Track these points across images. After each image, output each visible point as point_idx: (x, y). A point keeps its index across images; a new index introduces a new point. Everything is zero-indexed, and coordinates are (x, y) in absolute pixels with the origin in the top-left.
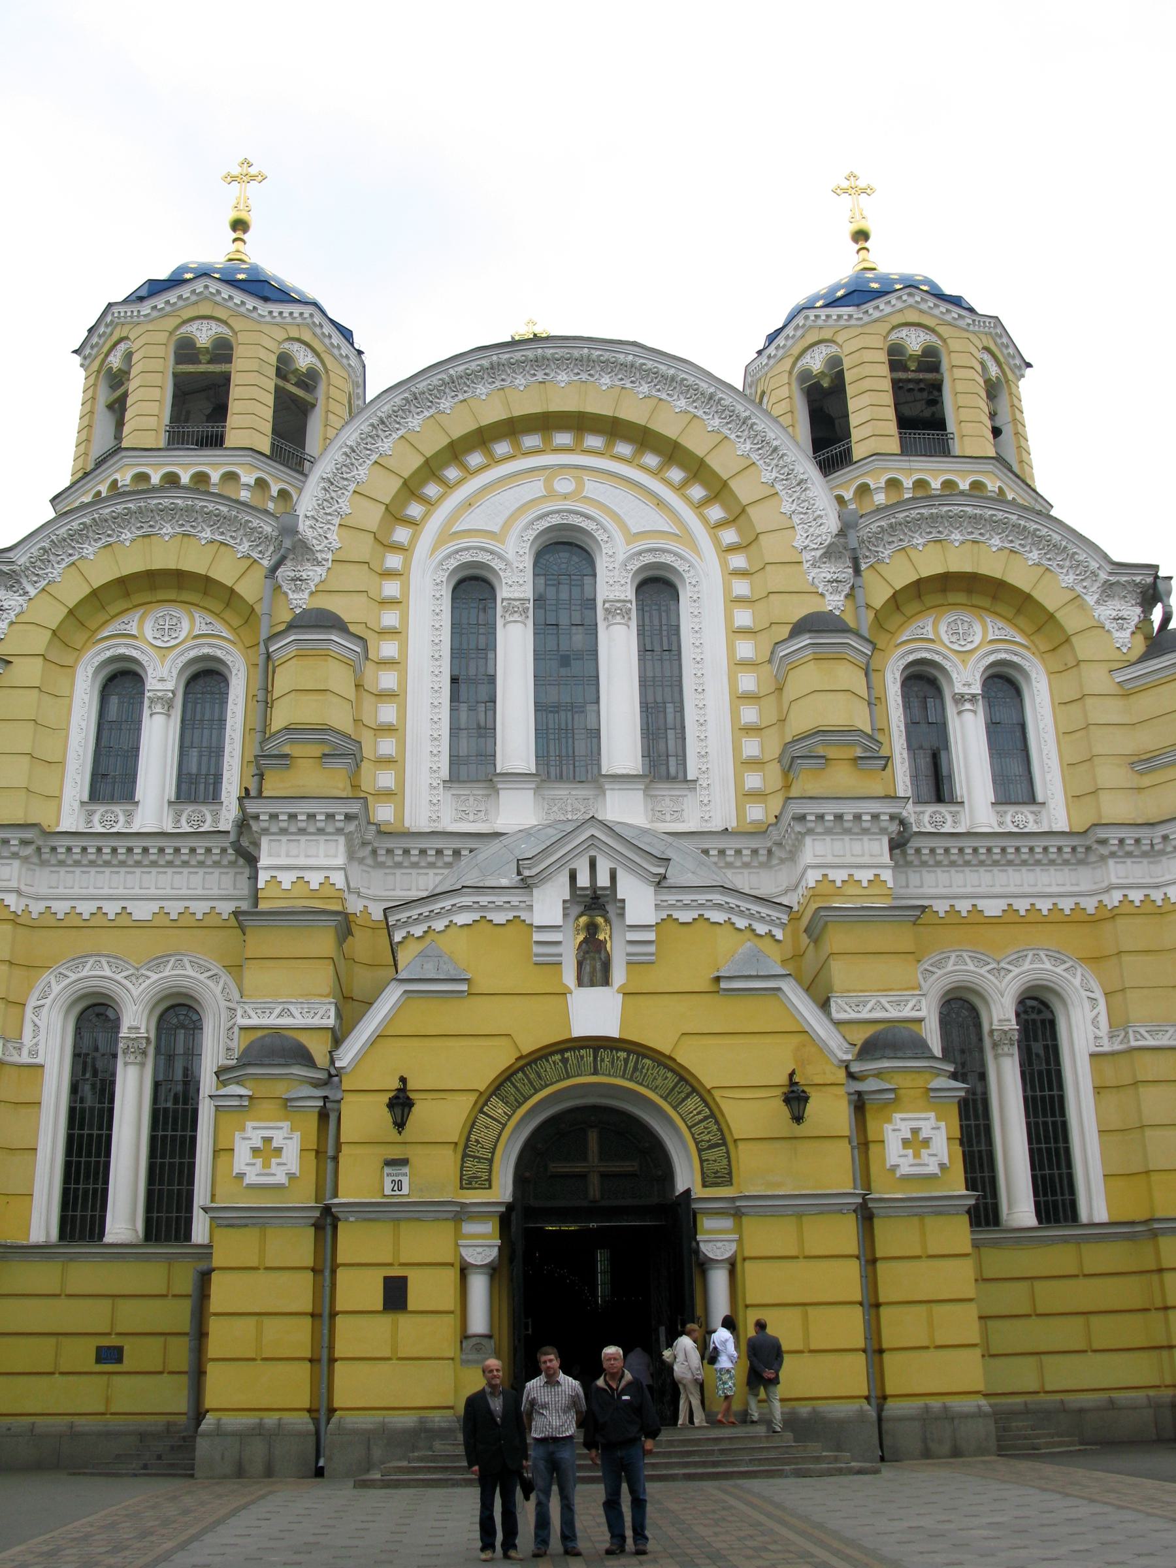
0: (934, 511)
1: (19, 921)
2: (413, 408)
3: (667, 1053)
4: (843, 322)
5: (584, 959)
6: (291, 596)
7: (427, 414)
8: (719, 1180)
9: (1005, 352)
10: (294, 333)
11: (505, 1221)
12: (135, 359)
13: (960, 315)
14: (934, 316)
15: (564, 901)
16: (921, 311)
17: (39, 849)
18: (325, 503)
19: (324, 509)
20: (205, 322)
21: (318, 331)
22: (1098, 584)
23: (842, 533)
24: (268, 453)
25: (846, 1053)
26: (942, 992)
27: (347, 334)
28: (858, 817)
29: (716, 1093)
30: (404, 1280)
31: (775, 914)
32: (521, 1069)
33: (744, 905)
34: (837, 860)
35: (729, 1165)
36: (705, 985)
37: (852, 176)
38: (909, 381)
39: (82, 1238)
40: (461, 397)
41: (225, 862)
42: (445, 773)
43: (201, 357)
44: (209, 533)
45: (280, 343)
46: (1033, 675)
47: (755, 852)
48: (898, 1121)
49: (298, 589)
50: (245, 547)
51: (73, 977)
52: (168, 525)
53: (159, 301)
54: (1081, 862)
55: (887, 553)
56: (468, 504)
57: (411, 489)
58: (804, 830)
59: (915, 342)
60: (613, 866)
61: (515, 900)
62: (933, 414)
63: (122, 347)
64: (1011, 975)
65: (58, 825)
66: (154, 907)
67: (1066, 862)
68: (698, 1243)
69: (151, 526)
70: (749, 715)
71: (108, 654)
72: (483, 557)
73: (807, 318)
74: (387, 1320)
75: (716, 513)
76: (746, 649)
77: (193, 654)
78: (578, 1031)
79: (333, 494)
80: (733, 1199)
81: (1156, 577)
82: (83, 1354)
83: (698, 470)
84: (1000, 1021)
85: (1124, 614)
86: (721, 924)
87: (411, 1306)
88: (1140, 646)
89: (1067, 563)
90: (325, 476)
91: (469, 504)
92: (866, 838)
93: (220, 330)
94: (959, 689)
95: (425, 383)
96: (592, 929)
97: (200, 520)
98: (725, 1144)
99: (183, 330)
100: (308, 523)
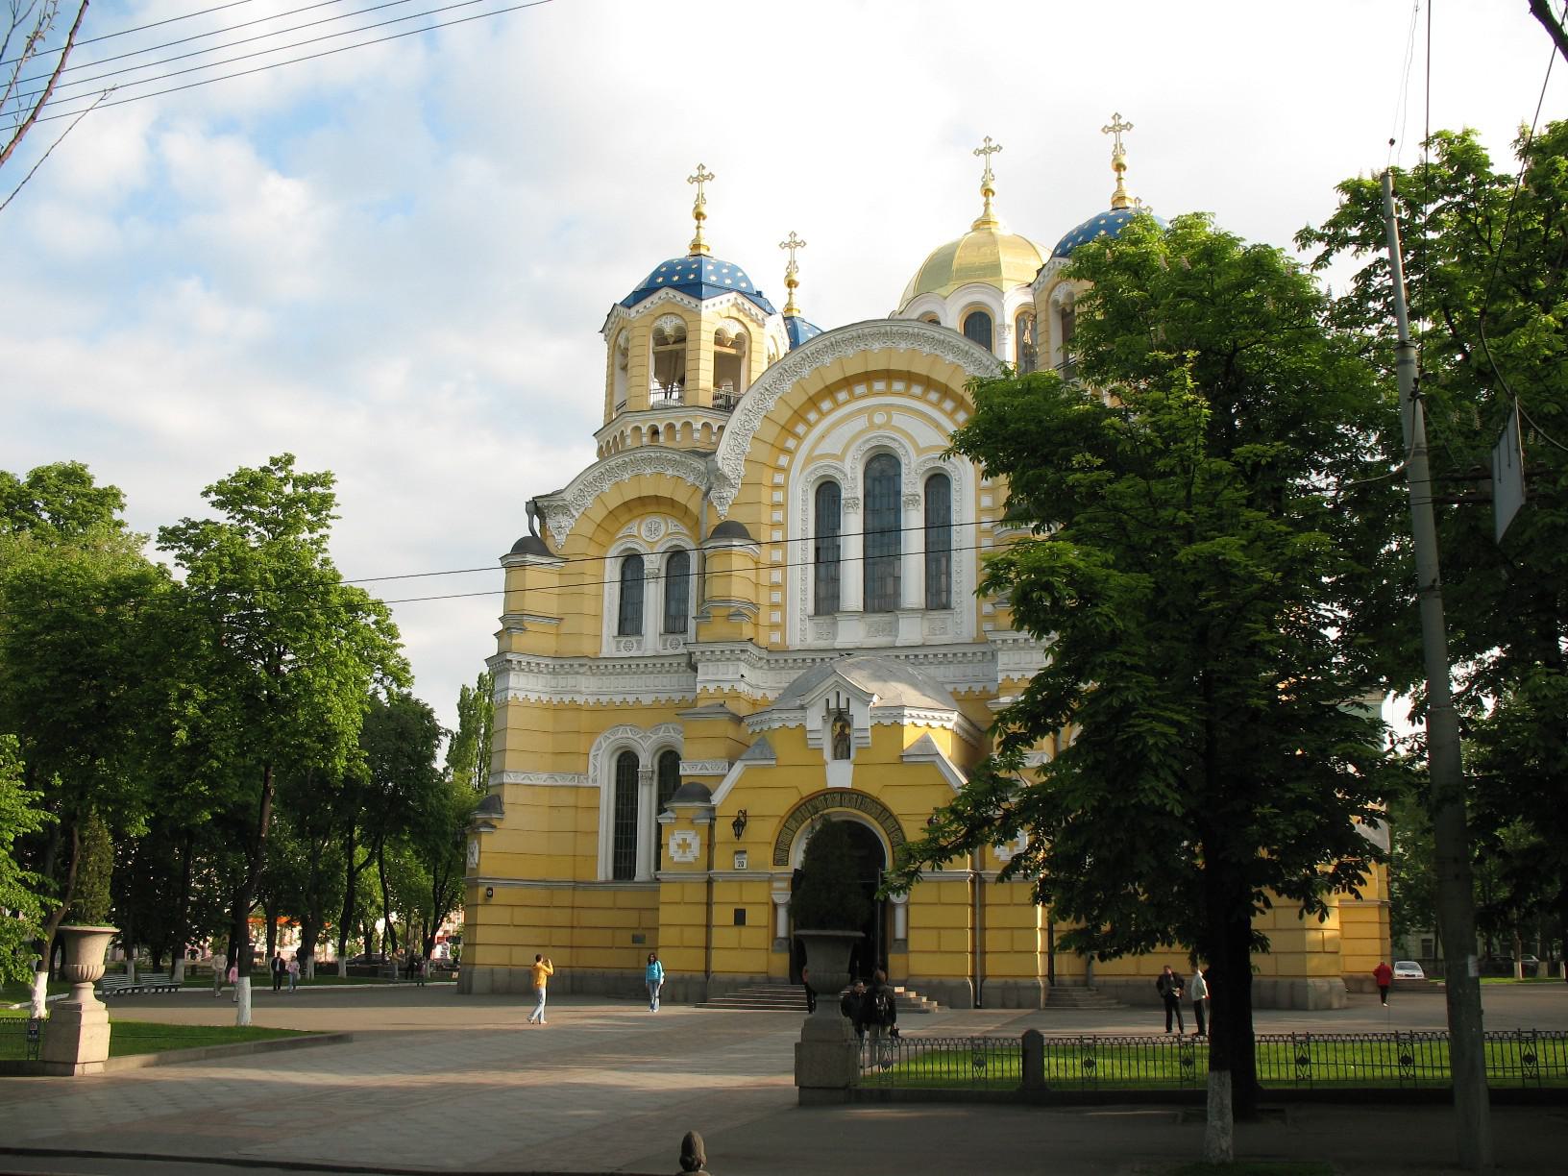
11: (793, 881)
32: (804, 804)
33: (922, 713)
37: (1117, 116)
49: (721, 504)
50: (691, 479)
51: (613, 738)
63: (624, 332)
66: (653, 697)
71: (622, 548)
72: (831, 472)
74: (735, 930)
78: (829, 786)
82: (625, 938)
96: (843, 728)
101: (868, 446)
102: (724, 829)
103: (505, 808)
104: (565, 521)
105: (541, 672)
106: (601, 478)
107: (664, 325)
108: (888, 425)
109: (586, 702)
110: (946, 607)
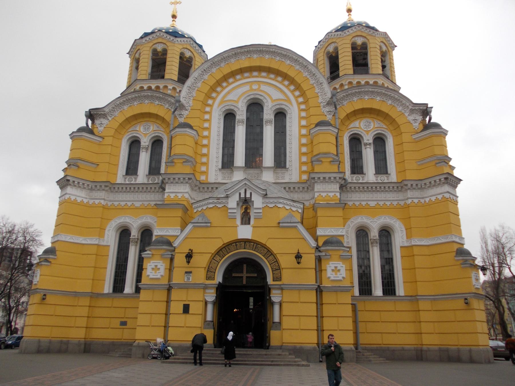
0: (360, 90)
1: (105, 207)
2: (213, 66)
3: (264, 243)
4: (338, 36)
5: (243, 217)
6: (179, 119)
7: (217, 68)
8: (278, 279)
9: (389, 42)
10: (185, 46)
12: (141, 54)
14: (365, 33)
15: (237, 201)
16: (362, 32)
17: (110, 188)
18: (189, 94)
20: (160, 44)
21: (192, 45)
22: (409, 110)
23: (332, 98)
24: (176, 79)
25: (315, 244)
26: (356, 228)
27: (200, 46)
28: (330, 178)
29: (278, 255)
30: (188, 305)
31: (298, 205)
32: (224, 247)
33: (288, 202)
34: (324, 190)
35: (281, 275)
36: (276, 225)
38: (358, 53)
39: (119, 292)
40: (227, 63)
41: (160, 191)
42: (220, 166)
43: (159, 54)
45: (181, 49)
46: (388, 137)
47: (303, 188)
48: (331, 264)
49: (181, 117)
51: (119, 222)
52: (146, 100)
53: (147, 38)
54: (400, 191)
55: (345, 103)
56: (229, 93)
57: (213, 89)
58: (314, 182)
59: (359, 41)
60: (251, 191)
61: (224, 201)
62: (365, 62)
63: (139, 51)
64: (377, 223)
65: (116, 181)
66: (141, 203)
67: (395, 191)
68: (270, 297)
69: (142, 101)
70: (304, 150)
71: (131, 136)
72: (232, 108)
73: (329, 36)
74: (184, 316)
75: (297, 93)
76: (304, 131)
77: (153, 135)
79: (191, 91)
80: (280, 285)
81: (427, 107)
82: (116, 323)
83: (292, 81)
84: (373, 236)
85: (417, 118)
86: (281, 208)
87: (191, 311)
88: (421, 127)
89: (400, 104)
90: (188, 86)
91: (229, 93)
92: (332, 184)
93: (163, 46)
94: (365, 141)
95: (216, 59)
96: (246, 209)
98: (280, 269)
99: (154, 46)
100: (184, 99)
101: (249, 98)
102: (180, 259)
103: (57, 253)
104: (104, 121)
105: (84, 188)
106: (123, 103)
108: (259, 89)
109: (107, 204)
110: (284, 167)
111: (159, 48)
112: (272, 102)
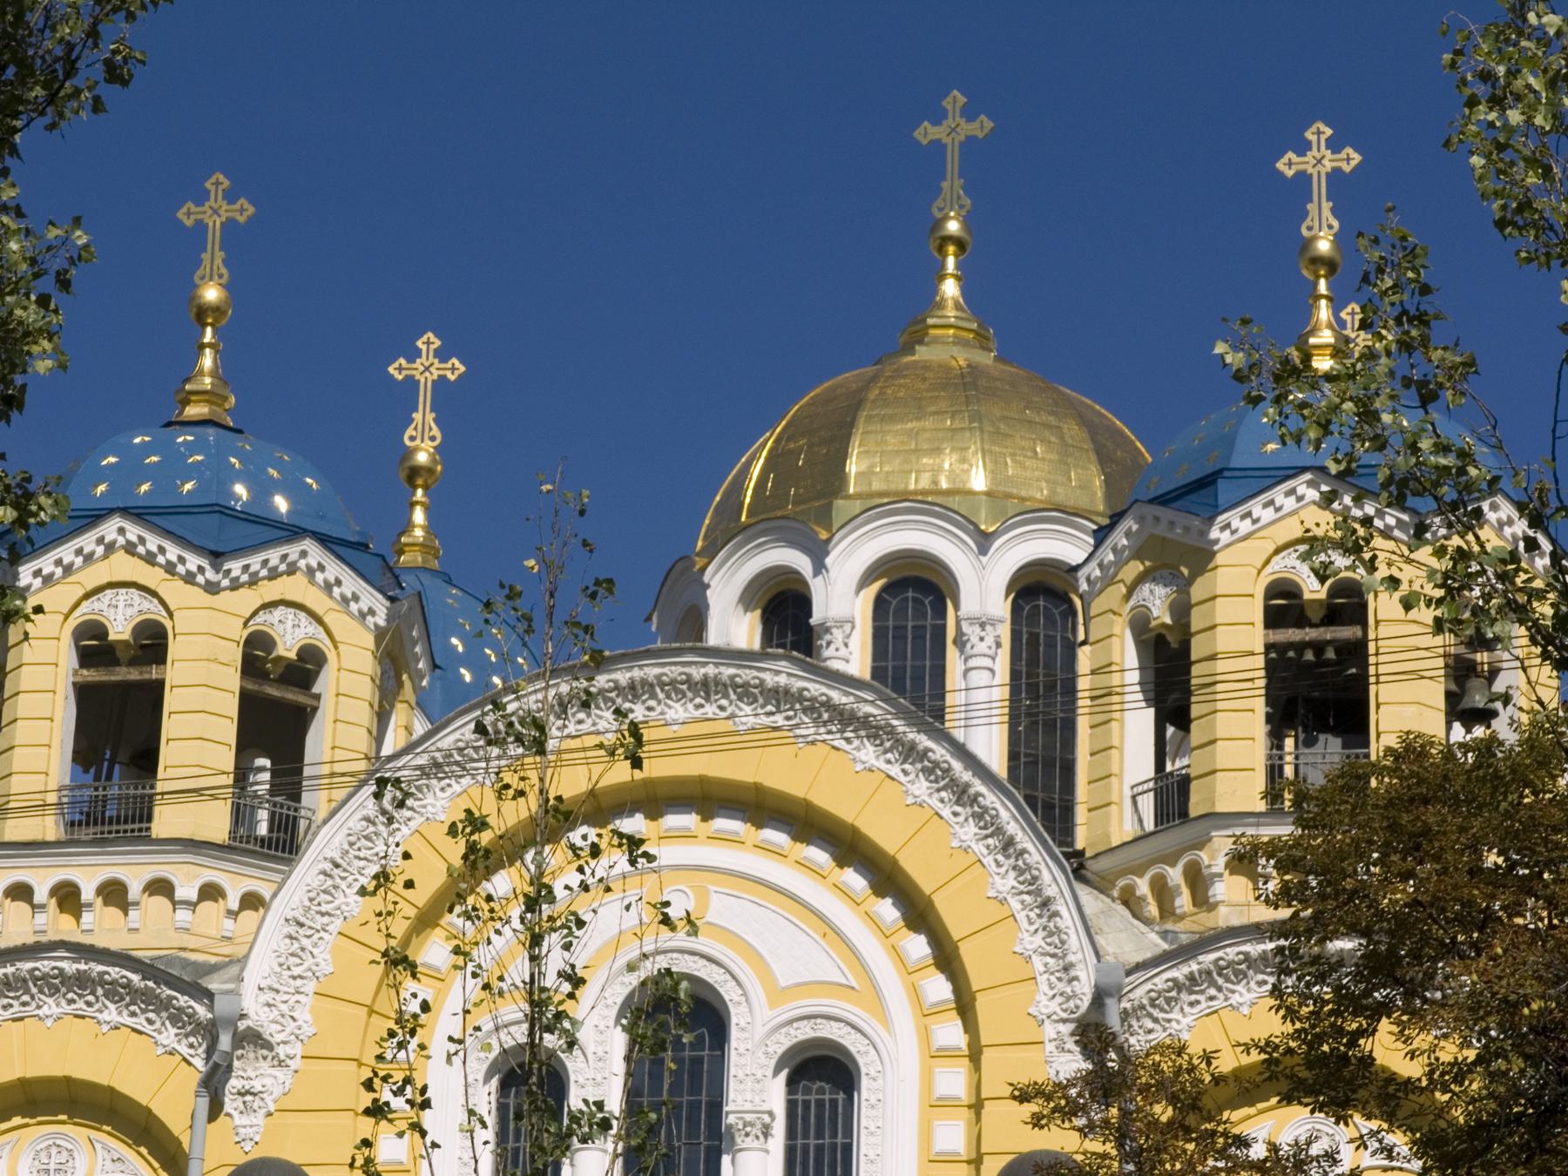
7: (457, 788)
13: (1399, 520)
19: (289, 969)
20: (123, 591)
44: (114, 1012)
49: (247, 1109)
55: (1185, 1021)
79: (306, 942)
97: (100, 991)
99: (85, 607)
107: (110, 613)
111: (120, 617)
112: (773, 1004)
